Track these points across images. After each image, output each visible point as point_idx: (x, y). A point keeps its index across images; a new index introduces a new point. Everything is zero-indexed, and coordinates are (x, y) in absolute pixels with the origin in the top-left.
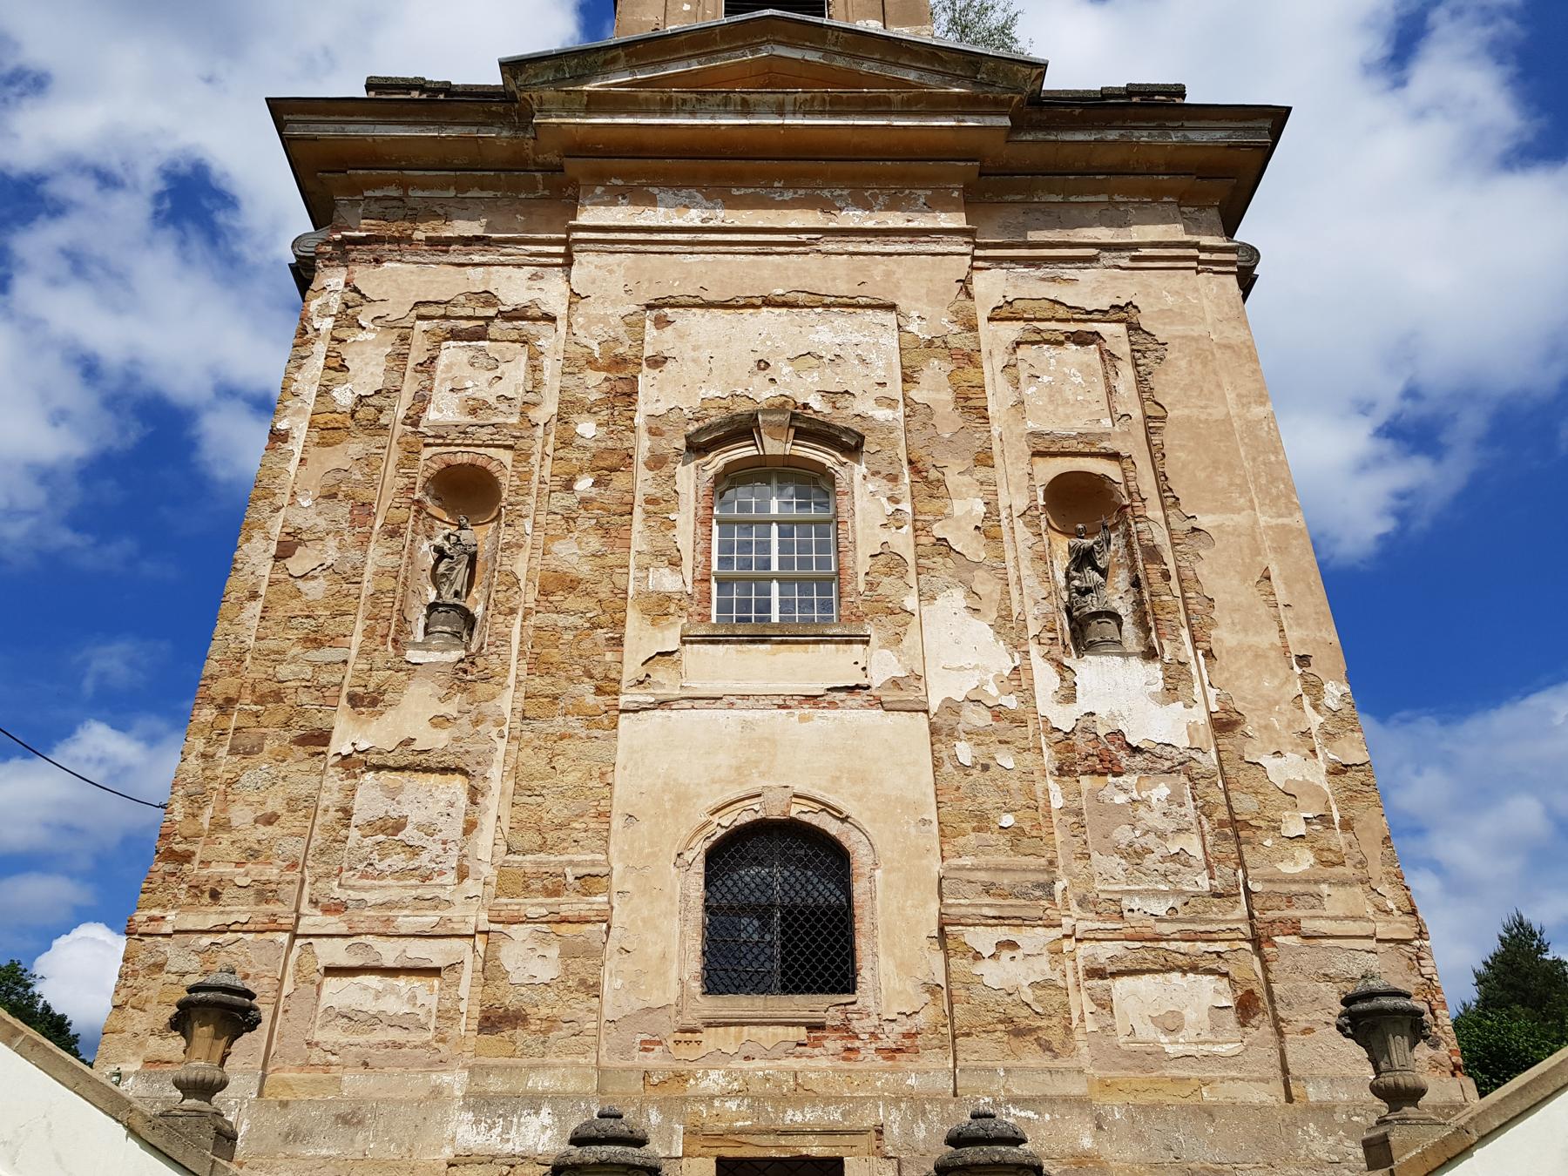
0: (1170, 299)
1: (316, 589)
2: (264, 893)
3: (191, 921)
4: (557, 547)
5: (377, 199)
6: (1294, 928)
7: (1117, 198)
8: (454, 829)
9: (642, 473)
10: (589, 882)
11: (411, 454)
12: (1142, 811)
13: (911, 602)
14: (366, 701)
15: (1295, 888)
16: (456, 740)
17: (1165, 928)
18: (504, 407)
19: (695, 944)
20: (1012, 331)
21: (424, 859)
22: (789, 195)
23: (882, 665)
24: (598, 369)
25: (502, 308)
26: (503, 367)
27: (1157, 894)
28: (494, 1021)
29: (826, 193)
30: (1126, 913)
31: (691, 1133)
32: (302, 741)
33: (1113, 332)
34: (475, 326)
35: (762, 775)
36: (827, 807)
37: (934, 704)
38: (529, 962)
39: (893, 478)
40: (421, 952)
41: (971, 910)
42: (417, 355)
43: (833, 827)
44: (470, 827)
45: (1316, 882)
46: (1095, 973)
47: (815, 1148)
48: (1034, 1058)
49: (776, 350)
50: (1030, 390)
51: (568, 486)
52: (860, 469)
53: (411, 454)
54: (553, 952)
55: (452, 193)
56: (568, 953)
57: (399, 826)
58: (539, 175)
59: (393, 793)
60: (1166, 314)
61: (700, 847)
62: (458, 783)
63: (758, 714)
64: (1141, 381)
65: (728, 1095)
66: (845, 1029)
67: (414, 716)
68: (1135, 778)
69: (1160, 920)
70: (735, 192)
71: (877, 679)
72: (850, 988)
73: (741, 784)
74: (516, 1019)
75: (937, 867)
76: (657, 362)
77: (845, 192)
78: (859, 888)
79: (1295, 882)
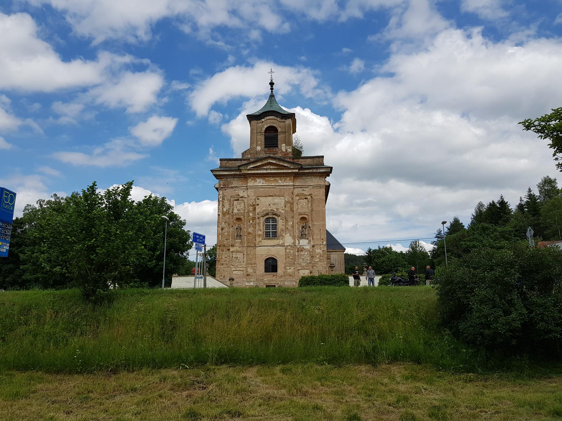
1: (226, 234)
11: (233, 216)
14: (232, 246)
20: (298, 198)
23: (281, 242)
28: (248, 275)
34: (238, 199)
38: (250, 270)
40: (241, 269)
42: (232, 204)
48: (291, 277)
53: (233, 216)
72: (276, 271)
76: (258, 205)
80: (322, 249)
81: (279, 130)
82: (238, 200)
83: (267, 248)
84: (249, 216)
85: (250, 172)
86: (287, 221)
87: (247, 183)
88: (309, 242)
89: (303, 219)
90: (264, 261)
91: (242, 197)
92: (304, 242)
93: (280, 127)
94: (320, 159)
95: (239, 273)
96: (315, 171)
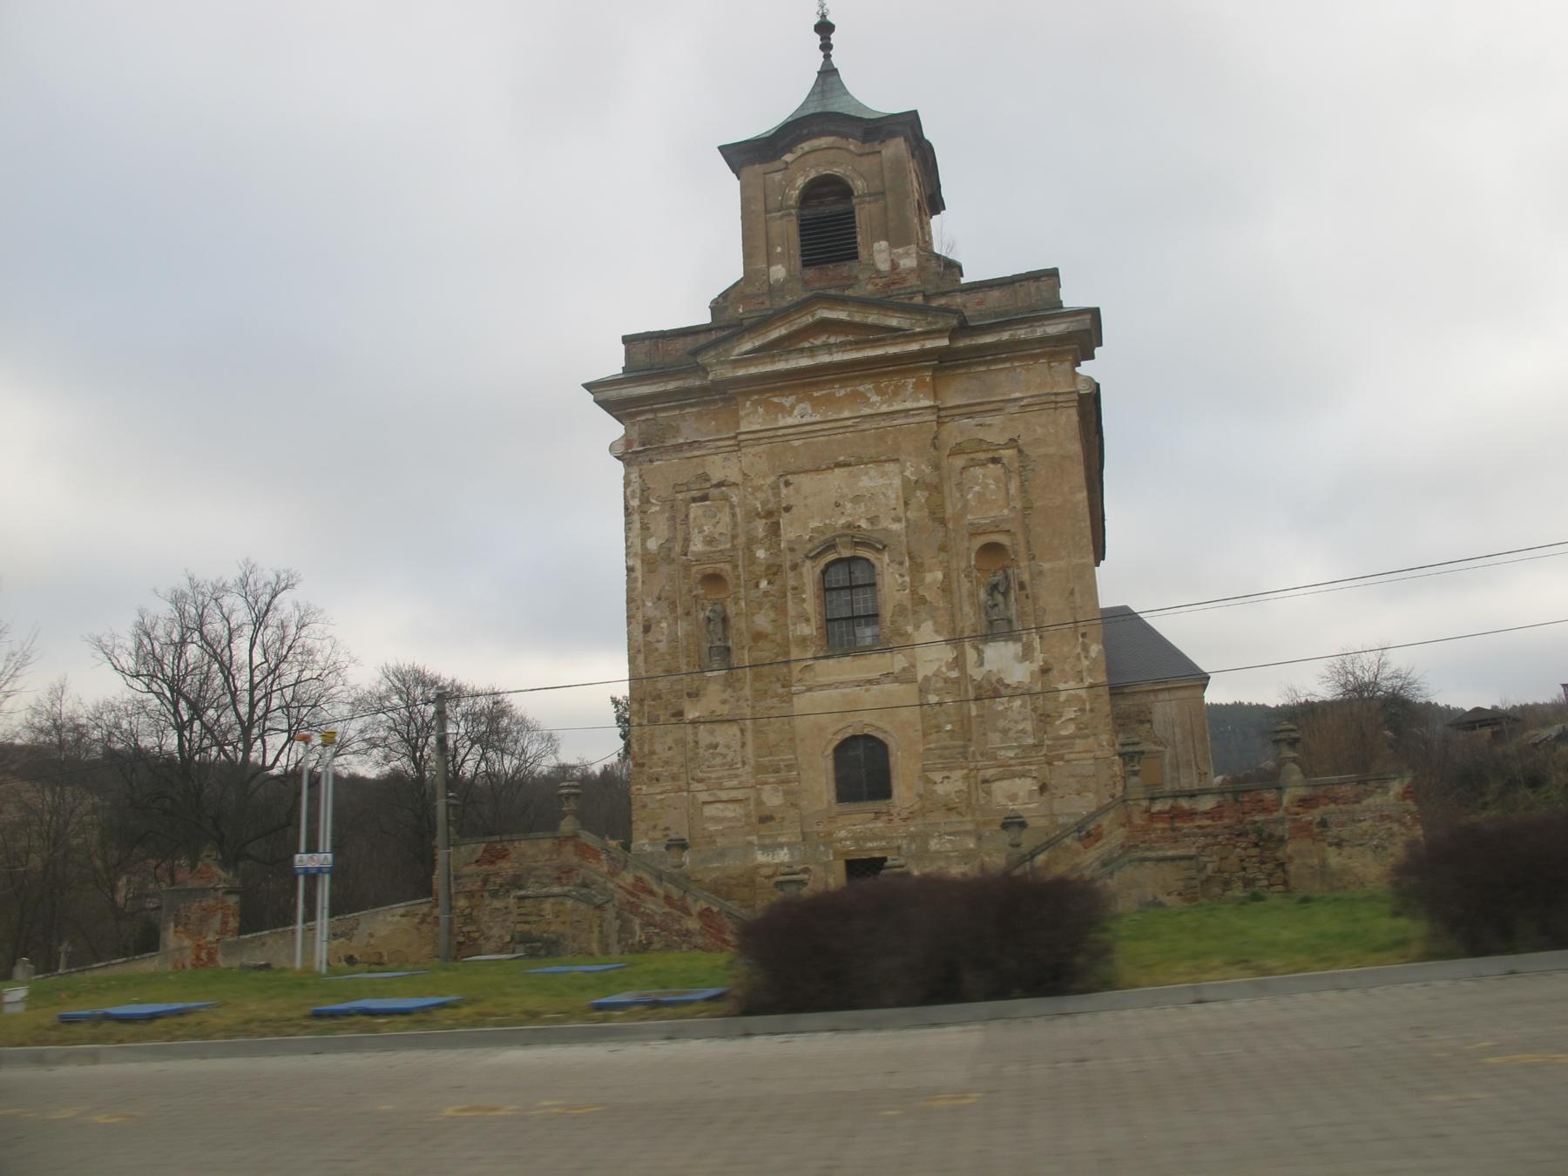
1: (663, 647)
2: (674, 778)
3: (652, 790)
4: (756, 618)
6: (1061, 758)
8: (737, 746)
9: (791, 574)
10: (790, 768)
13: (910, 629)
14: (694, 695)
19: (832, 786)
20: (959, 462)
22: (842, 392)
28: (764, 819)
29: (861, 388)
31: (835, 853)
32: (674, 715)
33: (1007, 454)
36: (878, 728)
37: (920, 678)
38: (773, 799)
39: (901, 564)
40: (734, 794)
43: (880, 736)
44: (743, 745)
46: (985, 781)
47: (877, 855)
48: (954, 818)
49: (843, 496)
51: (757, 585)
52: (886, 558)
53: (687, 567)
56: (786, 793)
57: (716, 746)
59: (712, 733)
61: (830, 750)
62: (735, 729)
64: (1022, 484)
65: (846, 839)
66: (889, 813)
67: (714, 699)
74: (770, 818)
75: (921, 749)
76: (788, 509)
78: (892, 759)
80: (1088, 681)
81: (859, 185)
82: (704, 498)
83: (838, 695)
84: (752, 560)
85: (741, 372)
86: (917, 568)
88: (1027, 655)
89: (992, 550)
91: (720, 484)
92: (1004, 661)
93: (862, 176)
94: (1044, 284)
95: (731, 811)
96: (1022, 333)
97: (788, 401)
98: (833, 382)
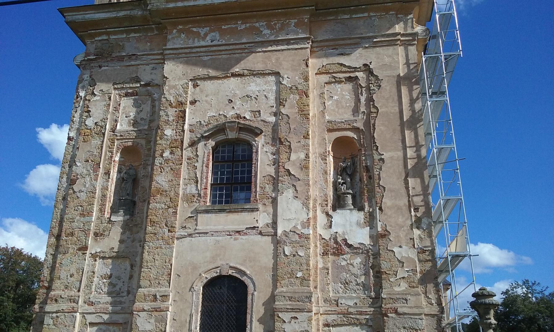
0: (387, 59)
5: (100, 40)
7: (372, 14)
12: (351, 267)
15: (398, 296)
16: (127, 247)
17: (351, 310)
18: (143, 122)
21: (117, 288)
22: (243, 27)
24: (172, 107)
25: (142, 83)
26: (143, 106)
27: (351, 298)
29: (257, 25)
30: (339, 305)
32: (79, 249)
35: (221, 260)
41: (283, 307)
45: (406, 294)
49: (235, 95)
50: (328, 103)
54: (152, 321)
55: (124, 36)
58: (153, 26)
60: (384, 66)
63: (220, 238)
68: (349, 256)
69: (351, 307)
70: (223, 27)
71: (260, 224)
73: (214, 263)
77: (264, 23)
79: (398, 294)
87: (165, 41)
90: (199, 288)
97: (202, 31)
98: (236, 19)
